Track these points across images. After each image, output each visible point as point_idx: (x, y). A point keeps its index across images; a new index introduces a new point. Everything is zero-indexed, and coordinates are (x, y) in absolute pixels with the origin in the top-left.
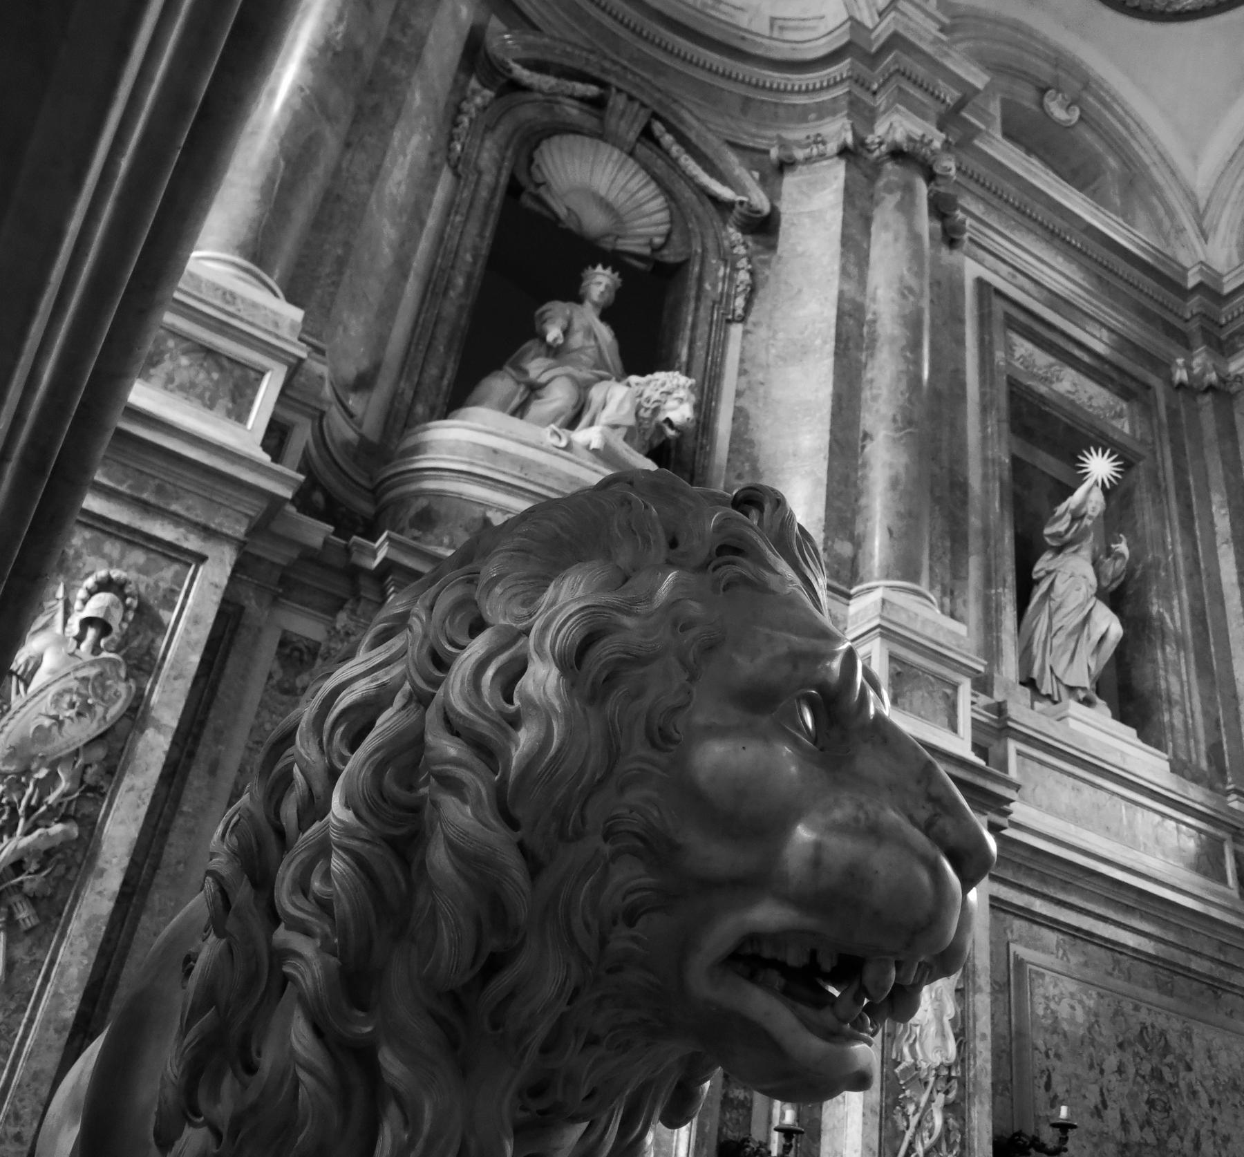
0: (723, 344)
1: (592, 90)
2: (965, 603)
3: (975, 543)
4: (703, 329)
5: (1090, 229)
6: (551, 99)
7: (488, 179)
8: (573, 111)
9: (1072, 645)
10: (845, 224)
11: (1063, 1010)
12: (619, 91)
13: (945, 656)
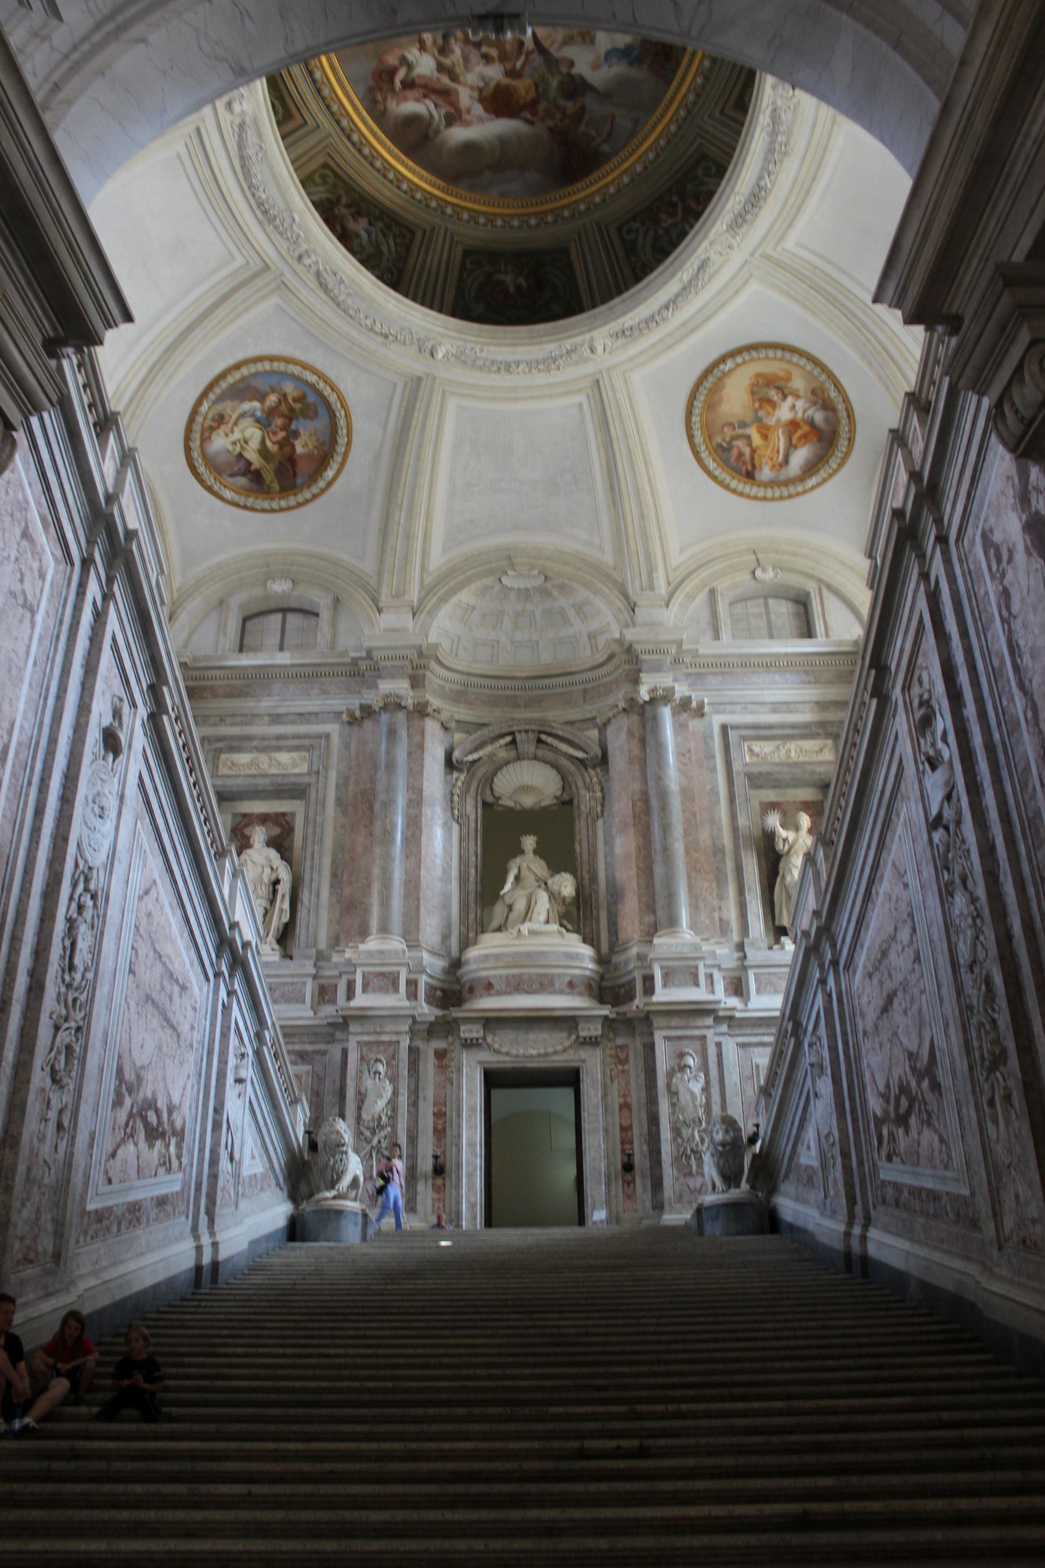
0: (595, 834)
5: (786, 655)
6: (491, 756)
7: (472, 817)
8: (503, 754)
10: (630, 751)
12: (520, 732)
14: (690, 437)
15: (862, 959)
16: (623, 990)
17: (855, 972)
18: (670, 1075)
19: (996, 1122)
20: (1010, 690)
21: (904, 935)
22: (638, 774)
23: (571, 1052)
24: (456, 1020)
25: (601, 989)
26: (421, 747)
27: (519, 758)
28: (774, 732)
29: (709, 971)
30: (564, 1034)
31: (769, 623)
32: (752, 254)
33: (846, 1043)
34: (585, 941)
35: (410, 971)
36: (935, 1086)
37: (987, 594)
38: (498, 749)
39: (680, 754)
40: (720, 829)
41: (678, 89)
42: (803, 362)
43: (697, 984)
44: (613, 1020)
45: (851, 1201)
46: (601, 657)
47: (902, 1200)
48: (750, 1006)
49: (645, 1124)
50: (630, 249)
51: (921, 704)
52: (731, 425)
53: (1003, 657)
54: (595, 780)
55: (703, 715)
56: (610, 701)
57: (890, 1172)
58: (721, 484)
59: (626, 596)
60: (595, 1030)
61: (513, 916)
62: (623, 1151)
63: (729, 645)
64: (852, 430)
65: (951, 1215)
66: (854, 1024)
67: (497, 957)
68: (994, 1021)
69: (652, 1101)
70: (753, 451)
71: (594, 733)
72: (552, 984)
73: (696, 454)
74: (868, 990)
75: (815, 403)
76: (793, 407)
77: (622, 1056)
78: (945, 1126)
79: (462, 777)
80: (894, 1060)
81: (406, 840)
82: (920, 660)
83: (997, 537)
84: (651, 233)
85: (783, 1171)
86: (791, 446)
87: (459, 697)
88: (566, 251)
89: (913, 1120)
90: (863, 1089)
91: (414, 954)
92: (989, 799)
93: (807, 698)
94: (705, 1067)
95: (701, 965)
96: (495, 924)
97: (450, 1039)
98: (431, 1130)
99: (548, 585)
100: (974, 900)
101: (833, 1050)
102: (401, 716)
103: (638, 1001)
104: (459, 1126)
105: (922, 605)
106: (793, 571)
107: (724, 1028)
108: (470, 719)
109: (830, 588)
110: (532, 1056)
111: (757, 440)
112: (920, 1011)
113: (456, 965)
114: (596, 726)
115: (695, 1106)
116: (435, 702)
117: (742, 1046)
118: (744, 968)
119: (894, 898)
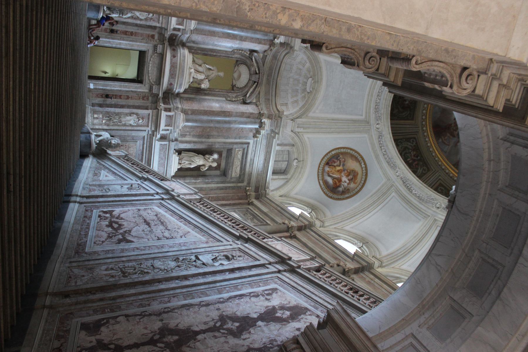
0: (221, 97)
1: (258, 72)
3: (200, 140)
4: (222, 93)
5: (268, 166)
6: (253, 65)
7: (233, 56)
8: (253, 69)
10: (246, 113)
11: (132, 149)
14: (344, 148)
15: (161, 211)
17: (159, 207)
18: (137, 114)
19: (106, 270)
20: (231, 292)
21: (167, 234)
22: (238, 114)
23: (148, 82)
24: (164, 44)
25: (168, 93)
26: (260, 43)
27: (250, 74)
28: (244, 159)
30: (154, 80)
31: (280, 161)
32: (394, 182)
33: (137, 200)
34: (185, 89)
35: (183, 29)
36: (119, 241)
37: (260, 286)
38: (255, 68)
39: (242, 129)
40: (215, 138)
41: (451, 168)
42: (358, 188)
43: (165, 126)
44: (157, 97)
45: (88, 197)
46: (279, 107)
47: (86, 220)
48: (157, 142)
50: (408, 140)
51: (233, 256)
52: (344, 161)
53: (240, 290)
54: (239, 99)
55: (254, 137)
56: (264, 108)
57: (96, 213)
58: (327, 154)
59: (297, 118)
60: (155, 91)
61: (197, 66)
62: (113, 95)
63: (275, 148)
64: (334, 199)
65: (80, 242)
66: (143, 204)
67: (184, 61)
68: (136, 273)
69: (129, 107)
70: (335, 166)
71: (254, 101)
72: (172, 78)
73: (338, 148)
74: (152, 214)
75: (345, 189)
76: (345, 182)
77: (145, 99)
78: (107, 244)
79: (248, 55)
80: (129, 223)
81: (229, 34)
82: (246, 257)
83: (274, 295)
84: (411, 148)
85: (100, 161)
86: (334, 178)
87: (275, 57)
88: (412, 119)
89: (110, 229)
90: (123, 206)
91: (189, 32)
92: (201, 280)
93: (253, 171)
94: (138, 126)
95: (172, 128)
96: (195, 59)
97: (158, 41)
98: (127, 30)
99: (306, 93)
100: (172, 269)
101: (136, 195)
102: (272, 38)
103: (162, 106)
104: (127, 40)
105: (262, 262)
106: (295, 172)
107: (150, 133)
108: (267, 60)
109: (287, 182)
110: (148, 68)
111: (338, 168)
112: (143, 238)
113: (183, 45)
114: (257, 102)
116: (274, 49)
117: (144, 137)
118: (169, 141)
119: (179, 231)
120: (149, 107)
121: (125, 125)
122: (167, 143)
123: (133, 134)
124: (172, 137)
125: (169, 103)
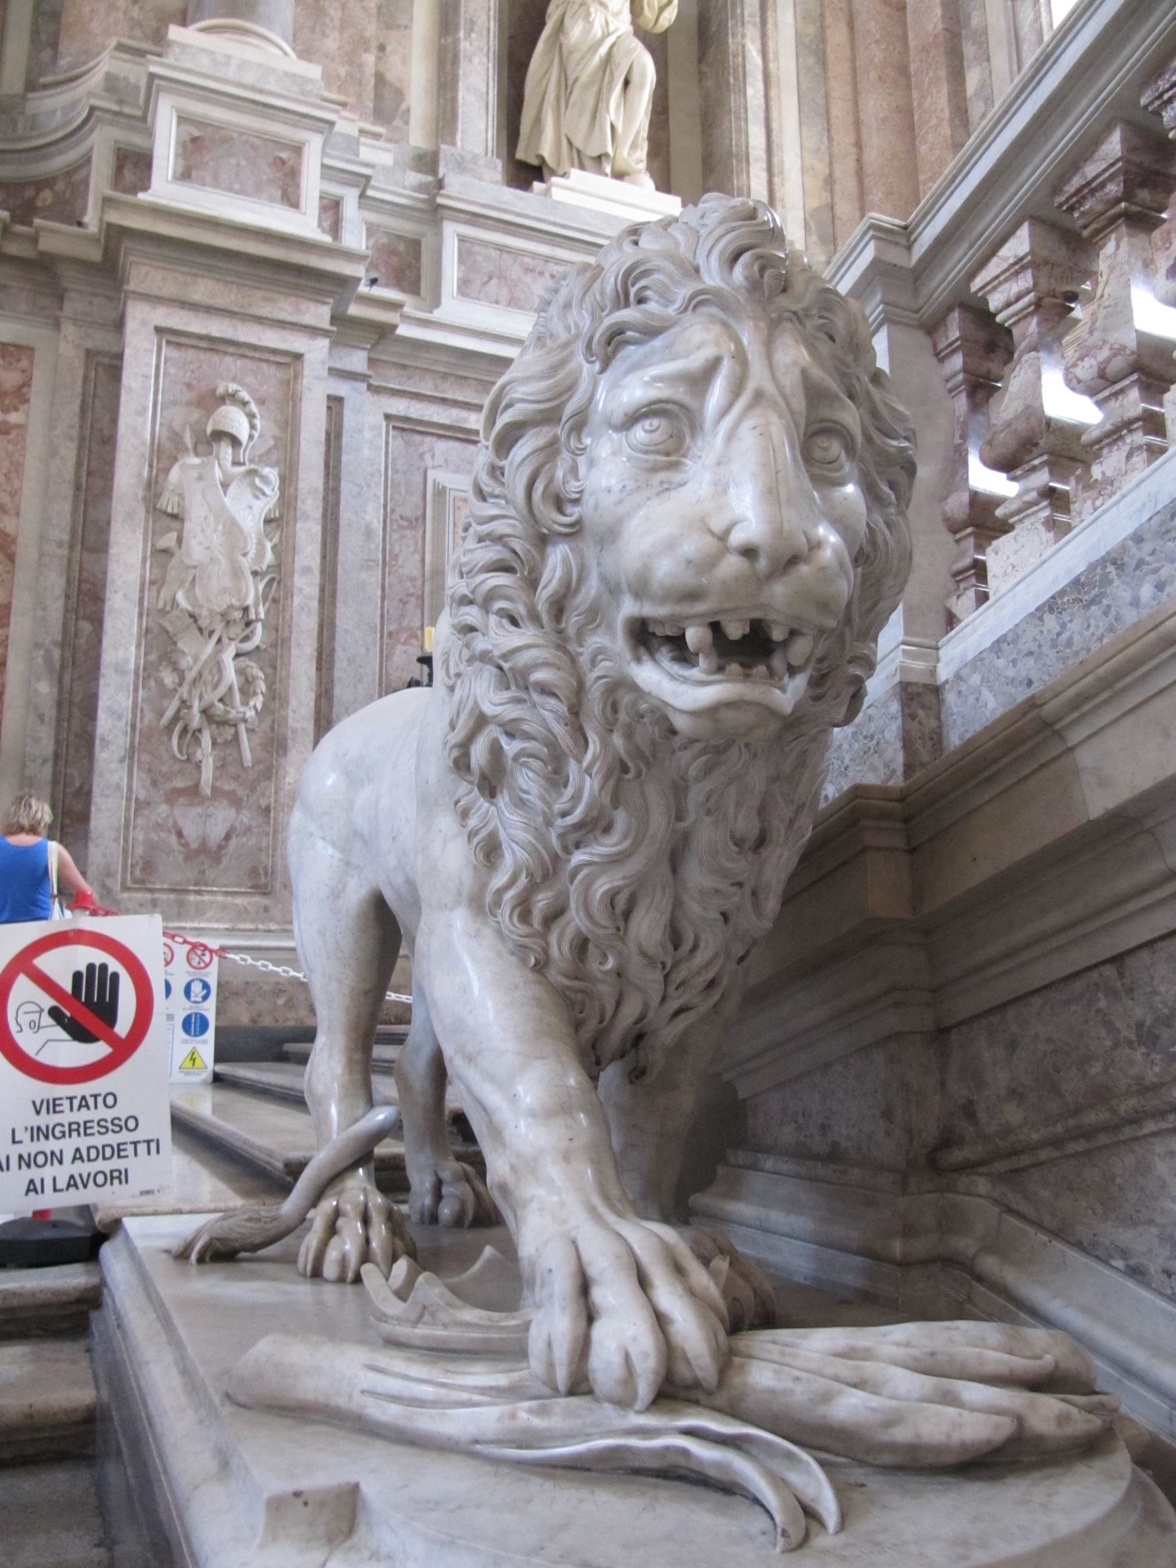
2: (405, 60)
9: (591, 103)
13: (266, 105)
16: (47, 196)
18: (163, 455)
29: (335, 189)
43: (291, 199)
49: (56, 610)
69: (90, 537)
95: (314, 145)
107: (357, 360)
115: (236, 573)
117: (401, 425)
120: (100, 340)
121: (277, 580)
122: (451, 231)
123: (373, 516)
124: (400, 186)
125: (70, 172)
